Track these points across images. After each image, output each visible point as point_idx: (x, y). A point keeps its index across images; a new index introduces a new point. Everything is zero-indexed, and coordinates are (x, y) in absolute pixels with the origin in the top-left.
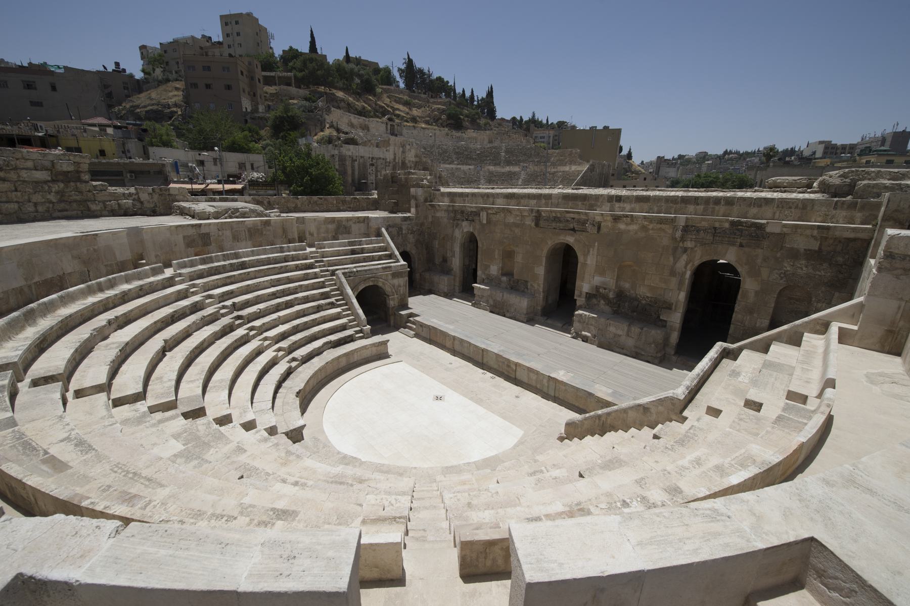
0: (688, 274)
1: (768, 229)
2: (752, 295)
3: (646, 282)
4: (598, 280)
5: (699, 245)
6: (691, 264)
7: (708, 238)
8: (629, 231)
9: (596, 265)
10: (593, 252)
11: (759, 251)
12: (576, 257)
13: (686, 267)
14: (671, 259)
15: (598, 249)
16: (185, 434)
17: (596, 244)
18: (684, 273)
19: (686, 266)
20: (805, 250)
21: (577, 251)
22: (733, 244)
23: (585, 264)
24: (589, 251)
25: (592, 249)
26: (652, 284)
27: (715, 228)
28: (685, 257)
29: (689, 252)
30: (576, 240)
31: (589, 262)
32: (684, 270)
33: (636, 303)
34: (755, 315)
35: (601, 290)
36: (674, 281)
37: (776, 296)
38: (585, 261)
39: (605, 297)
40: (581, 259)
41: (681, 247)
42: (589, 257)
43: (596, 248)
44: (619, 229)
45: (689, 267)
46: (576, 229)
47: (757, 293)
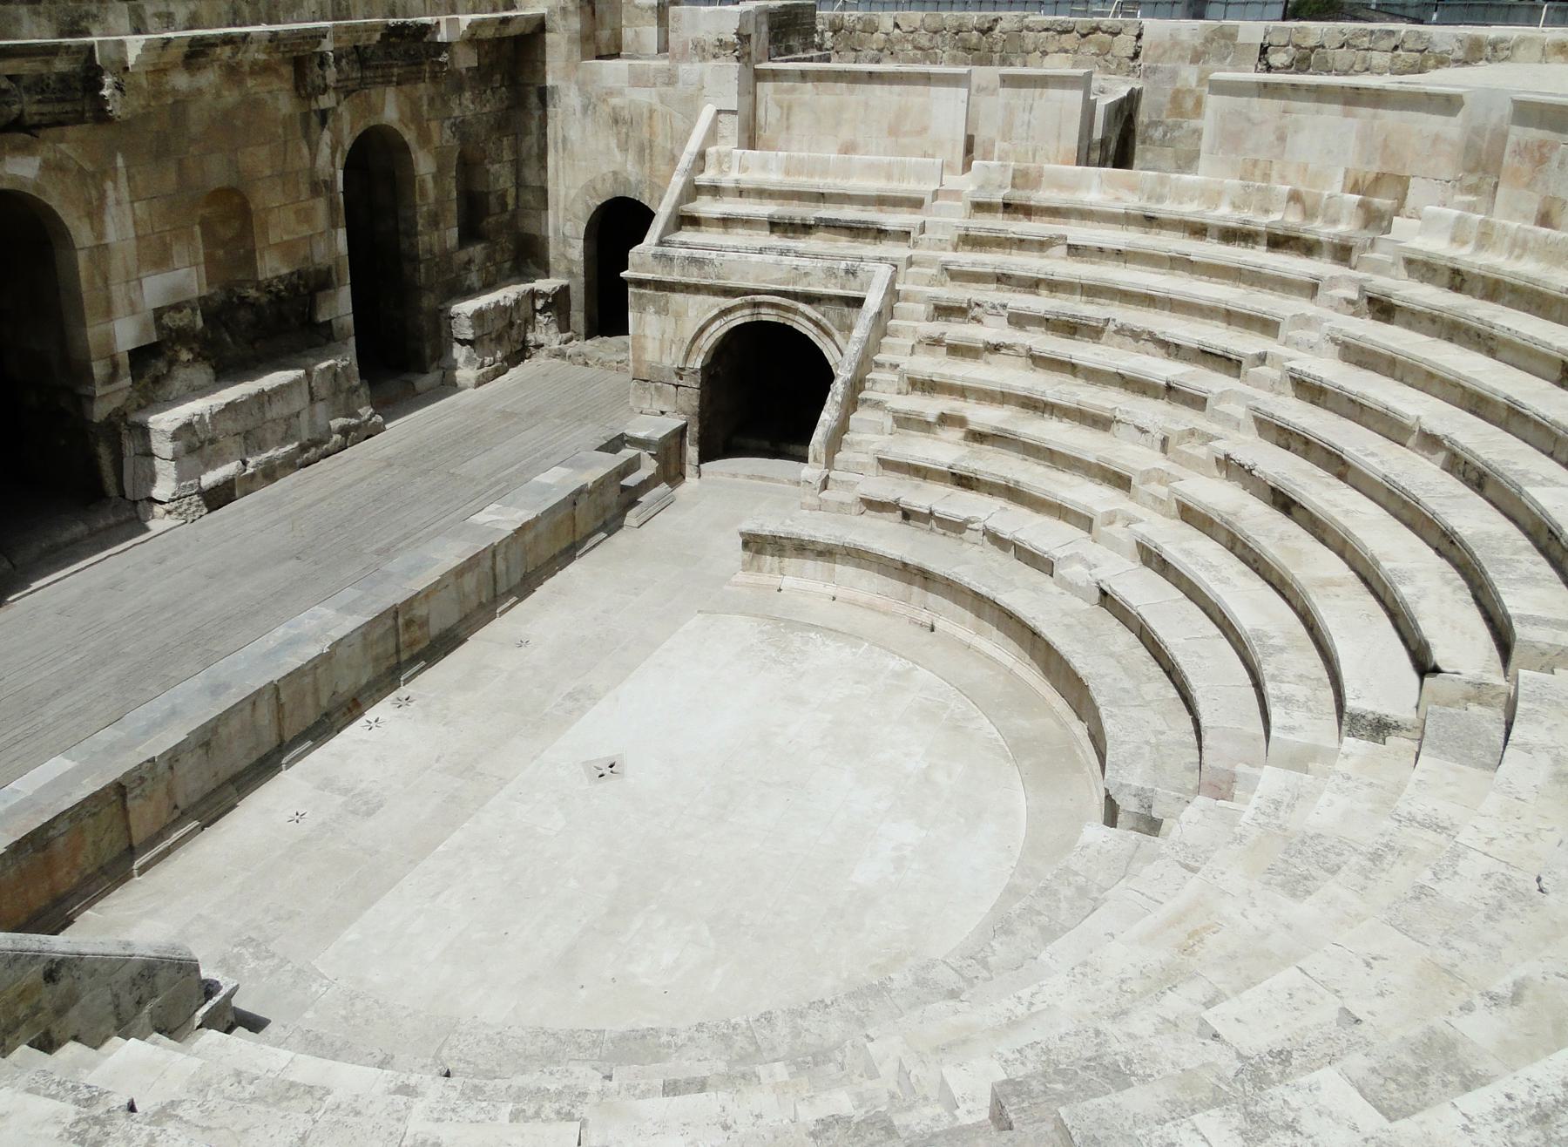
0: (340, 174)
1: (442, 36)
2: (430, 185)
3: (274, 237)
4: (156, 289)
5: (342, 97)
6: (340, 148)
7: (354, 75)
8: (200, 91)
9: (137, 237)
10: (117, 192)
11: (422, 86)
12: (63, 234)
13: (333, 164)
14: (305, 151)
15: (130, 178)
16: (1510, 576)
17: (120, 162)
18: (334, 181)
19: (329, 161)
20: (468, 69)
21: (60, 213)
22: (388, 83)
23: (101, 250)
24: (102, 196)
25: (109, 185)
26: (285, 238)
27: (356, 47)
28: (327, 136)
29: (330, 121)
30: (46, 166)
31: (112, 236)
32: (332, 169)
33: (244, 315)
34: (442, 226)
35: (166, 320)
36: (321, 205)
37: (454, 174)
38: (101, 235)
39: (182, 336)
40: (82, 235)
41: (315, 111)
42: (108, 219)
43: (123, 180)
44: (174, 90)
45: (338, 155)
46: (28, 120)
47: (435, 177)
